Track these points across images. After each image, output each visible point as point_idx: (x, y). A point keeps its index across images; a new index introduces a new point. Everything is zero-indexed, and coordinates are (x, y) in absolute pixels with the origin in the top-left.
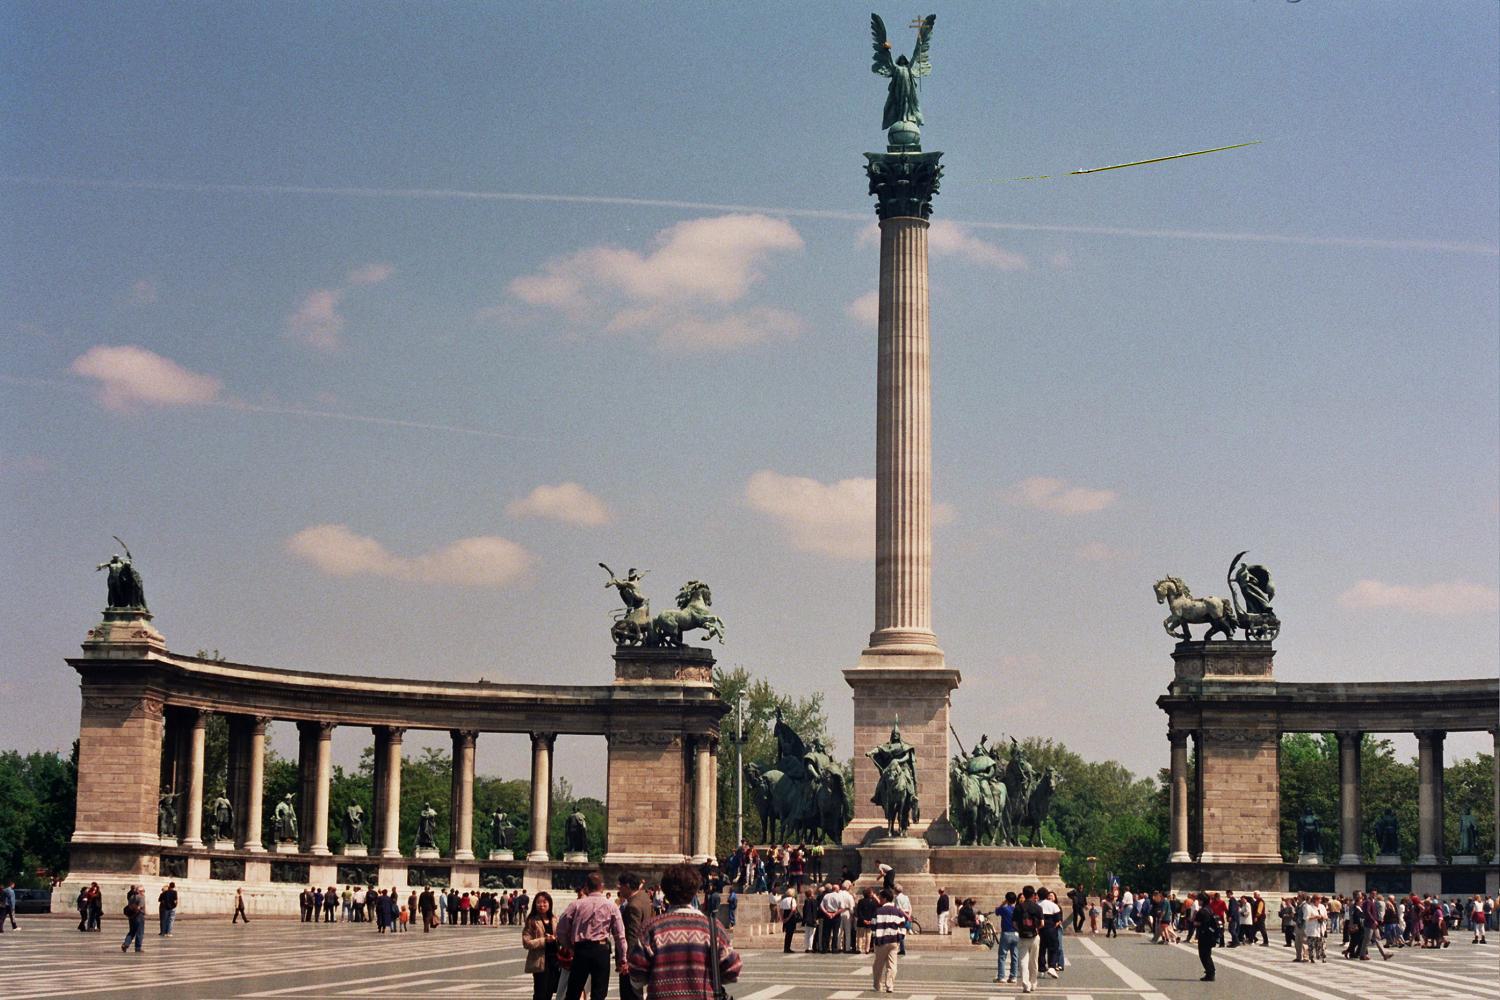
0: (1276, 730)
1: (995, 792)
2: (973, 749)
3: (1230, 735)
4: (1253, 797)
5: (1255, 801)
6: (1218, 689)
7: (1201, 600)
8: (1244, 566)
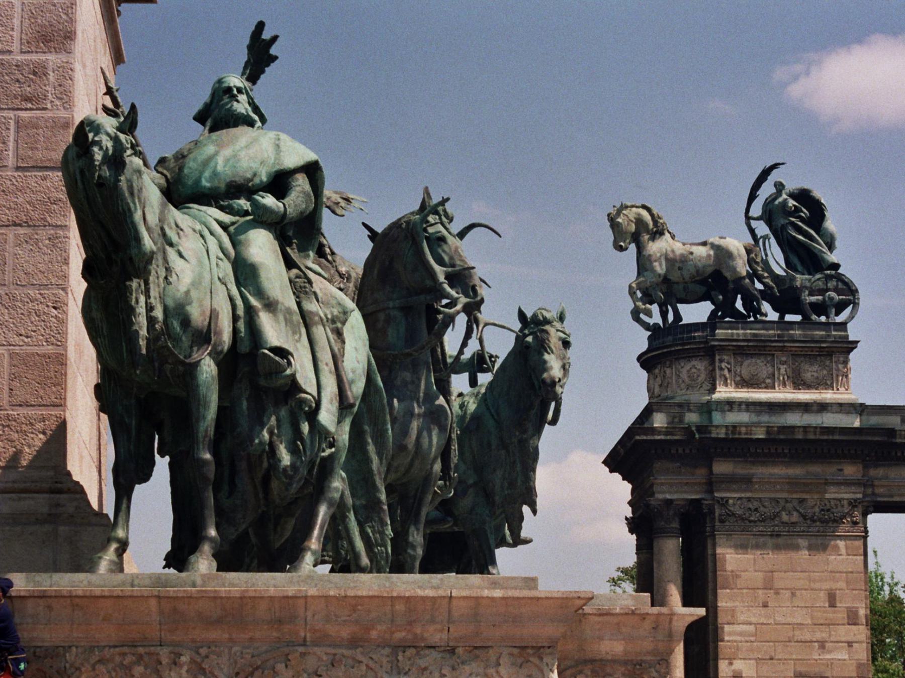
0: (861, 502)
1: (311, 306)
2: (203, 96)
3: (768, 510)
4: (819, 636)
5: (822, 645)
6: (744, 417)
7: (704, 244)
8: (779, 186)
